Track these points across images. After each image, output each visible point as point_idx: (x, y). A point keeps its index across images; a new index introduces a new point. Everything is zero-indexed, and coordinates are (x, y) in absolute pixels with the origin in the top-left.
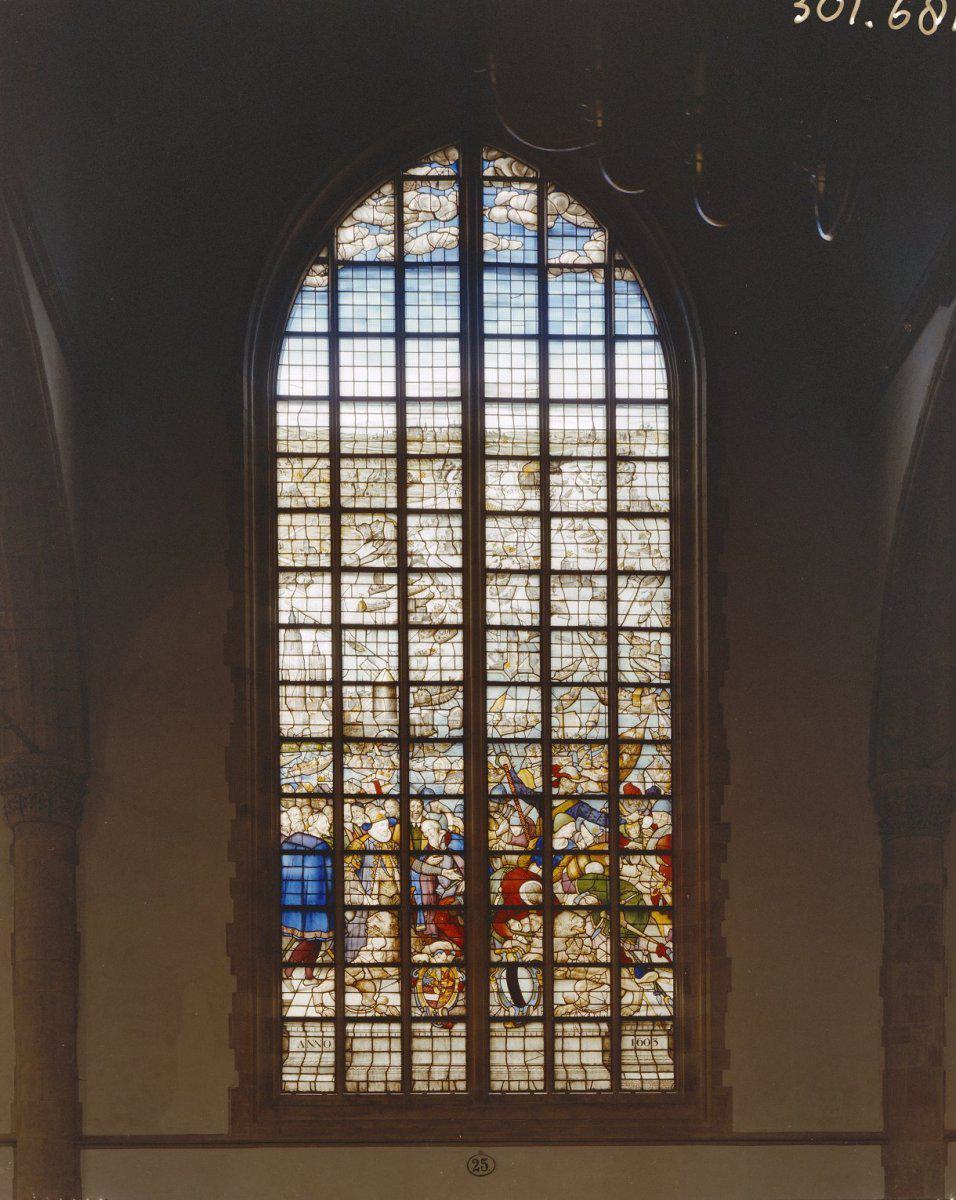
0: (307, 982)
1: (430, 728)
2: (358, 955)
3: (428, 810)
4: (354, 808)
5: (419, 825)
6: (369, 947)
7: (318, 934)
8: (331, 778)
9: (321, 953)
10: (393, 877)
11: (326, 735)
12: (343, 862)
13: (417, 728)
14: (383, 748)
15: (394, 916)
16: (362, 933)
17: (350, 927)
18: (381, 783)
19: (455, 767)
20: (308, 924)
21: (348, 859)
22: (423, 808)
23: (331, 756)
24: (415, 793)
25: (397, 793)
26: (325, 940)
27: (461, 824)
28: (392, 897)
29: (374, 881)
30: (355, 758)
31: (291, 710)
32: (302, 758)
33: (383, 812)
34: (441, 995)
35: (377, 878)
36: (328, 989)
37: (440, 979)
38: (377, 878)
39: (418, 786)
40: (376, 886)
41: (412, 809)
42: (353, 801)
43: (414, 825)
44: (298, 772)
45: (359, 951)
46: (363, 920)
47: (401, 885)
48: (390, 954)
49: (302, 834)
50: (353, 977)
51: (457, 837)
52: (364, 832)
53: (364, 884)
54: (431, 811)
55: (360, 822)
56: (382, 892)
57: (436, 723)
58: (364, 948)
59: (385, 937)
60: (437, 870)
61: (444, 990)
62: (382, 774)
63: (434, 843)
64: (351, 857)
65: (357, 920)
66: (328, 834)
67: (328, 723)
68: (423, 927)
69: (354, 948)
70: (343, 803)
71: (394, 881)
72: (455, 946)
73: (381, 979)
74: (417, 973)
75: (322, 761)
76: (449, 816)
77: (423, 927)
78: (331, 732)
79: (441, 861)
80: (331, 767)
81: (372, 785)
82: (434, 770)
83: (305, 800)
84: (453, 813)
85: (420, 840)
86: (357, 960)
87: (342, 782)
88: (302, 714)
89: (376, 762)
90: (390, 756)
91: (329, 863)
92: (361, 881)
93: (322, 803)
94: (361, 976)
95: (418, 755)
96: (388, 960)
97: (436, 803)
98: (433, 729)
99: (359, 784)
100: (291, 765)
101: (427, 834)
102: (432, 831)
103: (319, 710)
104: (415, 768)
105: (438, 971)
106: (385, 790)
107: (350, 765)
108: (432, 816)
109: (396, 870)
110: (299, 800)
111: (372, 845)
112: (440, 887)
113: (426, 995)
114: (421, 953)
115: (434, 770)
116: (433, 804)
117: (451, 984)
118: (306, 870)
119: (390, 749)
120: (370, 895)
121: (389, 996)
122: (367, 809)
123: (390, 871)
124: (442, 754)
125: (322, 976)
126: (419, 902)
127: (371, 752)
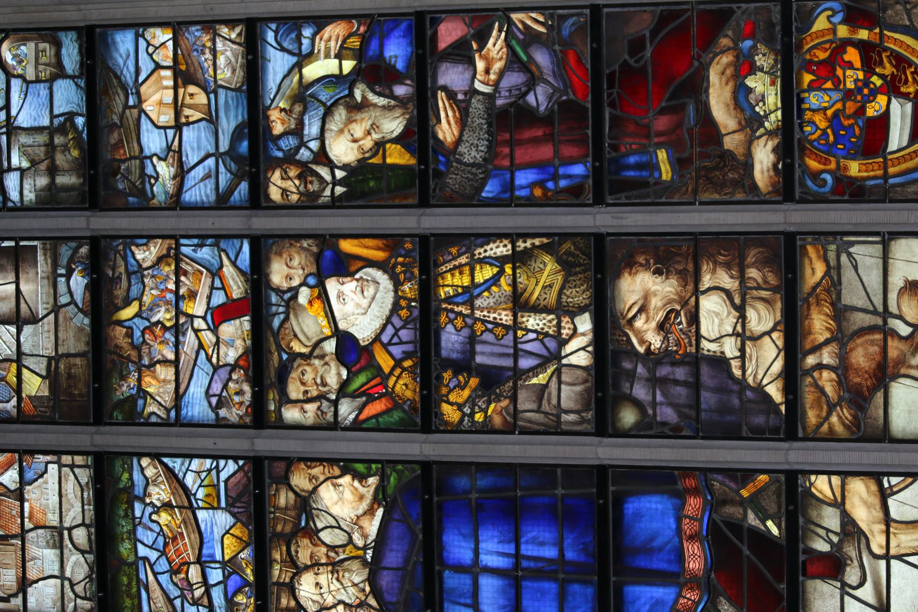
0: (852, 575)
1: (58, 140)
2: (760, 390)
3: (289, 143)
4: (294, 391)
5: (340, 174)
6: (730, 348)
7: (688, 527)
8: (208, 462)
9: (752, 519)
10: (501, 261)
11: (84, 476)
12: (457, 429)
13: (61, 180)
14: (120, 293)
15: (630, 265)
16: (680, 373)
17: (668, 414)
18: (219, 299)
19: (165, 56)
20: (659, 563)
21: (450, 413)
22: (290, 159)
23: (145, 462)
24: (244, 186)
25: (246, 248)
26: (715, 504)
27: (334, 32)
28: (567, 266)
29: (516, 326)
30: (151, 386)
31: (24, 584)
32: (153, 555)
33: (304, 295)
34: (893, 88)
35: (506, 318)
36: (876, 501)
37: (836, 96)
38: (506, 318)
39: (224, 178)
40: (533, 322)
41: (294, 198)
42: (272, 395)
43: (339, 190)
44: (194, 573)
45: (742, 383)
46: (640, 369)
47: (525, 236)
48: (753, 273)
49: (374, 570)
50: (831, 408)
51: (374, 45)
52: (363, 362)
53: (525, 363)
54: (298, 131)
55: (334, 375)
56: (551, 298)
57: (46, 122)
58: (735, 364)
59: (697, 293)
60: (477, 105)
61: (878, 82)
62: (193, 295)
63: (394, 125)
64: (446, 408)
65: (640, 392)
66: (373, 481)
67: (53, 469)
68: (662, 155)
69: (736, 402)
70: (281, 425)
71: (519, 259)
72: (725, 42)
73: (840, 313)
74: (815, 176)
75: (160, 493)
76: (312, 71)
77: (662, 155)
78: (79, 460)
79: (451, 95)
80: (176, 464)
81: (228, 329)
82: (178, 127)
83: (277, 556)
84: (304, 58)
85: (384, 166)
86: (775, 392)
87: (220, 424)
88: (33, 550)
89: (163, 315)
90: (140, 271)
91: (462, 482)
92: (518, 374)
93: (284, 498)
94: (827, 379)
95: (135, 176)
96: (772, 280)
97: (274, 115)
98: (61, 130)
99: (223, 373)
100: (174, 592)
101: (368, 143)
102: (358, 130)
103: (19, 495)
104: (170, 186)
105: (814, 100)
106: (237, 288)
107: (167, 398)
108: (312, 129)
109: (480, 252)
110: (276, 570)
111: (405, 334)
112: (531, 98)
113: (893, 145)
114: (748, 165)
115: (178, 127)
116: (278, 129)
117: (852, 55)
118: (489, 560)
119: (122, 269)
120: (564, 343)
121: (897, 281)
122: (297, 348)
123: (484, 274)
124: (131, 103)
125: (831, 519)
126: (578, 170)
127: (130, 334)
